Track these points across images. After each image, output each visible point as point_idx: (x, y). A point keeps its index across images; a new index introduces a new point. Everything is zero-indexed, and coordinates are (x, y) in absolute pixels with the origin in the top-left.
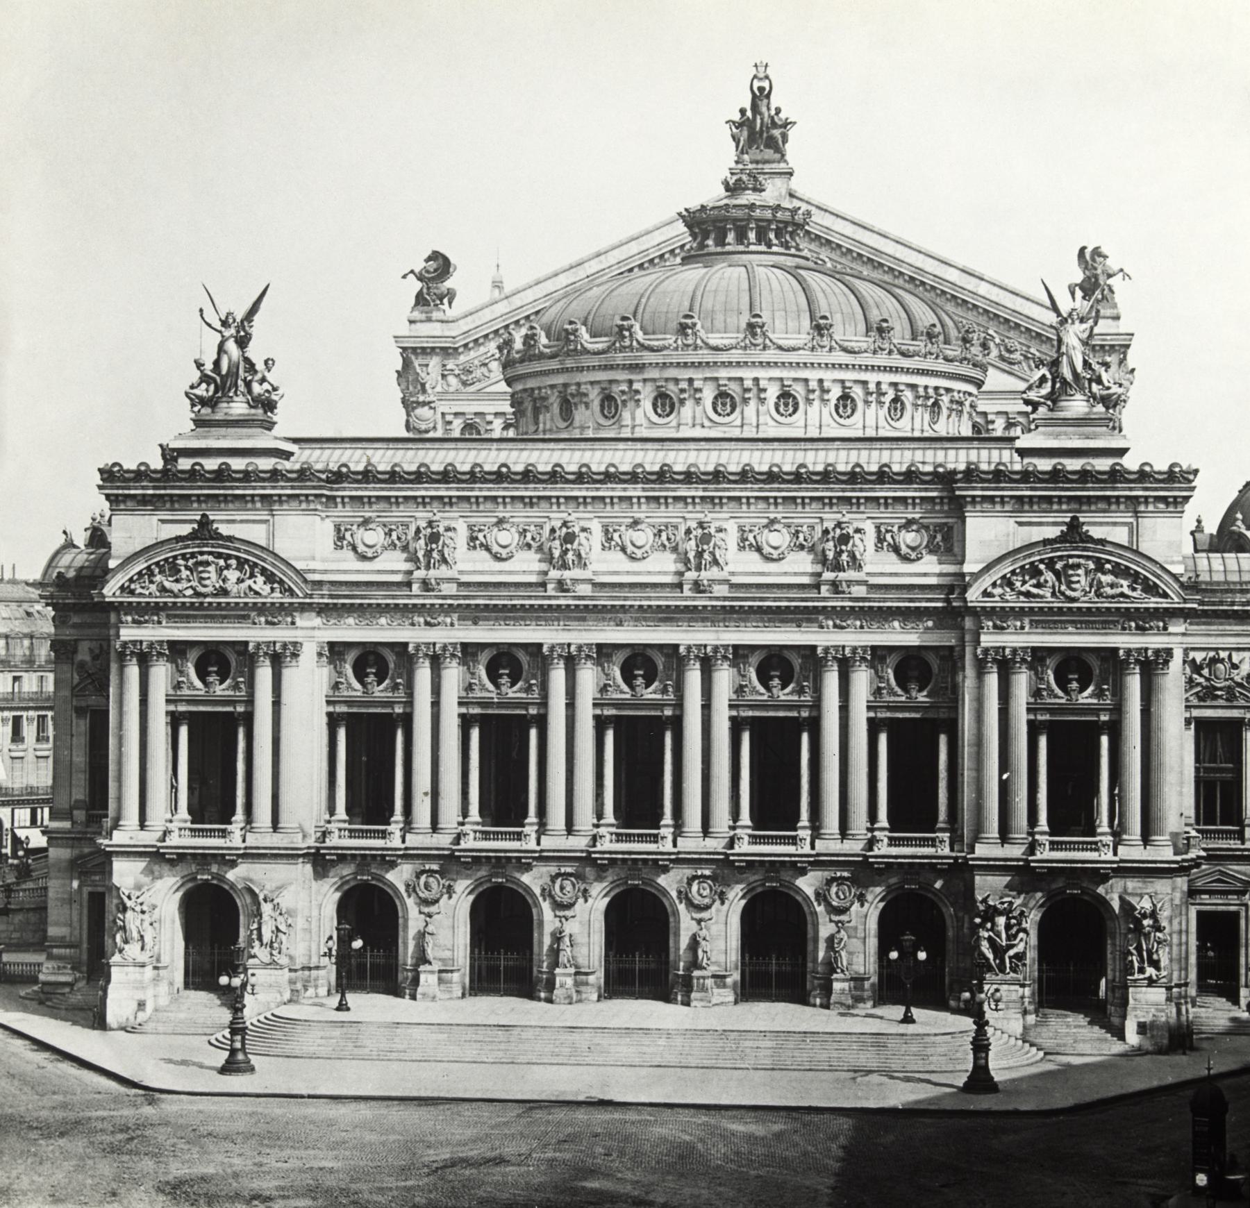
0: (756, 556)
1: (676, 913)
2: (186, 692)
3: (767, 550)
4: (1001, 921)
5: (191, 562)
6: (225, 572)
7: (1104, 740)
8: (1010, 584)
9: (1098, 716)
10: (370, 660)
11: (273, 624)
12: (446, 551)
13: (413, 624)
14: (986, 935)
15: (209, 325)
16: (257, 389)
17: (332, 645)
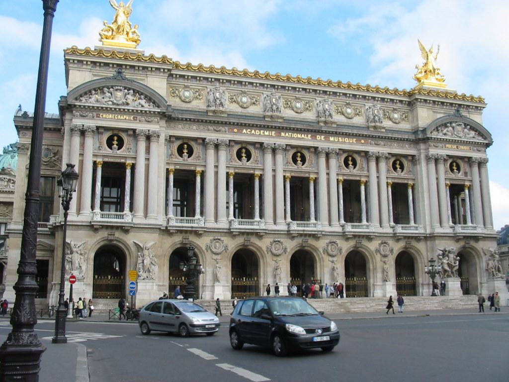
0: (343, 116)
1: (321, 259)
2: (101, 152)
3: (346, 115)
4: (452, 256)
5: (111, 89)
6: (128, 96)
7: (467, 191)
8: (438, 130)
9: (465, 182)
10: (185, 147)
11: (149, 122)
12: (223, 101)
13: (208, 130)
14: (447, 262)
15: (112, 6)
16: (131, 35)
17: (170, 136)
